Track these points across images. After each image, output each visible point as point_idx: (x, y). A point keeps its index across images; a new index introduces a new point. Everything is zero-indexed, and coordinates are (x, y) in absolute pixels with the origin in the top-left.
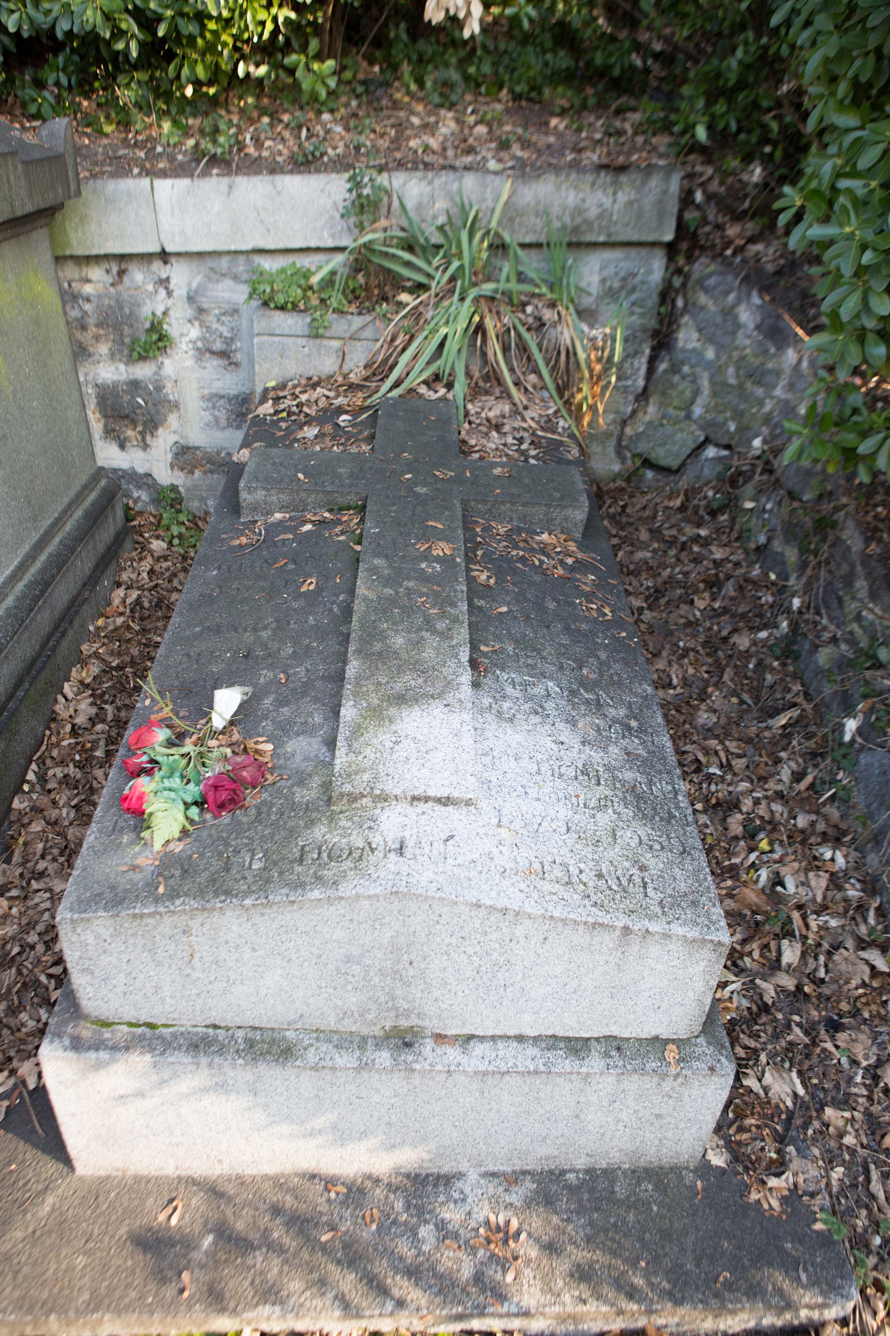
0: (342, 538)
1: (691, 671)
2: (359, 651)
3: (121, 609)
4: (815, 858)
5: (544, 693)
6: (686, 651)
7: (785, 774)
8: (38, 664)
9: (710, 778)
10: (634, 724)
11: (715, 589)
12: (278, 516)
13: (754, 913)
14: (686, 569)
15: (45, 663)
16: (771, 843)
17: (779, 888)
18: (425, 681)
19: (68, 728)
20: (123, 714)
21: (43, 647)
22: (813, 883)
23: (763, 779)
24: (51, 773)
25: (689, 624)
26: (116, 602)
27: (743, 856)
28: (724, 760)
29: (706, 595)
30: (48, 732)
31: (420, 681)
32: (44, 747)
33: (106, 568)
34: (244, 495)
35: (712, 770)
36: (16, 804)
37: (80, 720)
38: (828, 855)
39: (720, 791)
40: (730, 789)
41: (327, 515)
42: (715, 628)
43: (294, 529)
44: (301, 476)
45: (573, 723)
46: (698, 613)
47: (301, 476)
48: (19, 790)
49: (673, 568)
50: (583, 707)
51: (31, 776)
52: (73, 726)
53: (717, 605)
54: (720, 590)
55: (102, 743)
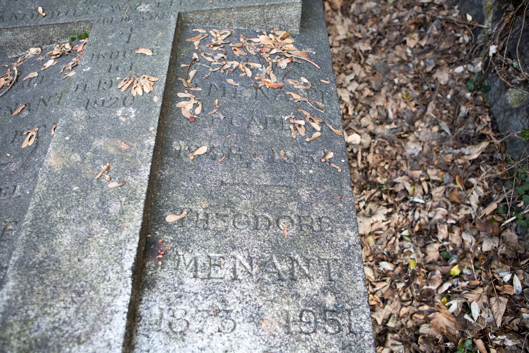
1: (403, 105)
2: (20, 263)
4: (497, 282)
5: (229, 275)
6: (401, 86)
7: (474, 200)
9: (414, 205)
10: (330, 301)
11: (422, 30)
13: (446, 340)
14: (401, 14)
16: (461, 268)
17: (466, 317)
18: (77, 312)
22: (494, 308)
23: (457, 205)
25: (402, 62)
27: (438, 284)
28: (426, 190)
29: (416, 35)
31: (73, 309)
35: (416, 200)
38: (507, 277)
39: (422, 216)
40: (430, 215)
42: (422, 63)
44: (40, 9)
45: (256, 319)
46: (409, 51)
47: (40, 9)
49: (391, 14)
50: (272, 288)
53: (423, 43)
54: (426, 29)
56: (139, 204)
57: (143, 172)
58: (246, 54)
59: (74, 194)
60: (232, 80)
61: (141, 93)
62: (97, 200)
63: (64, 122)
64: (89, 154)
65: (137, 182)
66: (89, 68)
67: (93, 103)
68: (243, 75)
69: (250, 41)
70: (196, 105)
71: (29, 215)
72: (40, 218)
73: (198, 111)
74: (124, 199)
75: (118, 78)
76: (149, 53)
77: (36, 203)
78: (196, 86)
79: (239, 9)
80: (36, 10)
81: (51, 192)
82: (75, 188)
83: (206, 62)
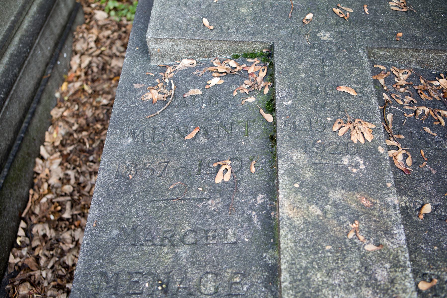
0: (251, 99)
3: (78, 73)
8: (14, 148)
12: (186, 63)
15: (20, 146)
19: (45, 186)
20: (82, 179)
21: (16, 133)
24: (34, 230)
26: (75, 67)
30: (31, 192)
32: (29, 204)
33: (63, 45)
34: (151, 45)
36: (12, 260)
37: (54, 181)
41: (233, 63)
43: (202, 82)
44: (205, 21)
47: (205, 21)
48: (13, 244)
51: (21, 232)
52: (49, 185)
55: (68, 206)
56: (407, 272)
57: (398, 235)
58: (431, 99)
59: (329, 254)
60: (428, 129)
61: (362, 141)
62: (358, 264)
63: (286, 165)
64: (328, 207)
65: (395, 247)
66: (290, 102)
67: (310, 146)
68: (437, 123)
69: (431, 85)
70: (405, 156)
71: (285, 276)
72: (300, 280)
73: (409, 161)
74: (388, 265)
75: (329, 119)
76: (353, 93)
77: (288, 261)
78: (398, 134)
79: (428, 51)
80: (200, 20)
81: (300, 249)
82: (328, 248)
83: (397, 105)
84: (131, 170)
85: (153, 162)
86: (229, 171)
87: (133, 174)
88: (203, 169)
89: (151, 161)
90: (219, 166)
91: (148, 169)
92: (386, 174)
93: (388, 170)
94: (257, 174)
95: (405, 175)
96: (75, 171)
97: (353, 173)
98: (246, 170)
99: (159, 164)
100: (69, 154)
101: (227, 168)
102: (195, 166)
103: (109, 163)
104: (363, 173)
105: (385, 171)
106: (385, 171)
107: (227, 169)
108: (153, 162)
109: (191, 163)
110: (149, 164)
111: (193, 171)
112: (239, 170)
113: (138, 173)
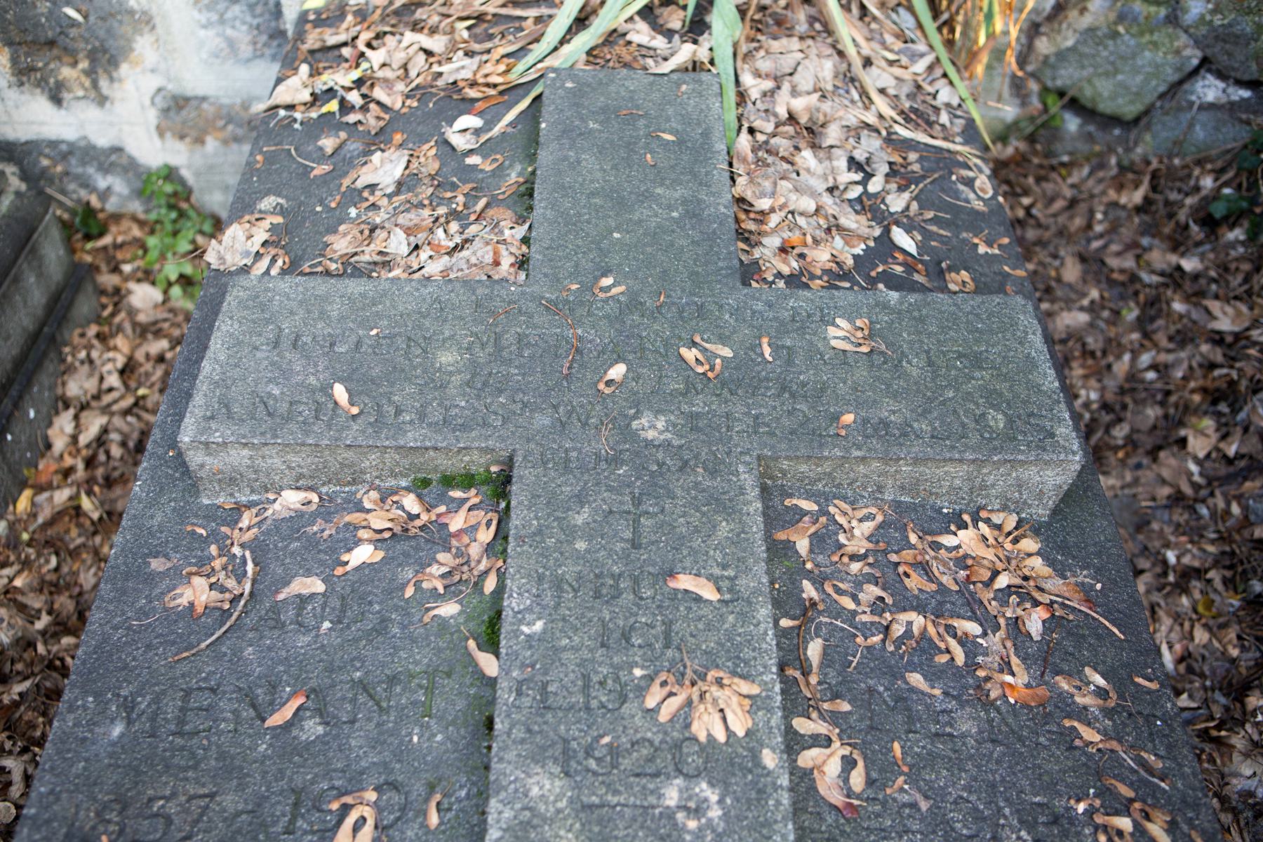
0: (449, 609)
1: (1201, 636)
3: (69, 461)
6: (1188, 574)
11: (1223, 407)
12: (292, 499)
14: (1164, 358)
25: (1178, 498)
26: (59, 444)
29: (1208, 423)
33: (28, 384)
34: (195, 458)
41: (411, 503)
42: (1235, 509)
43: (325, 555)
44: (340, 392)
46: (1193, 468)
47: (340, 392)
49: (1135, 355)
53: (1232, 450)
54: (1235, 411)
58: (934, 587)
60: (918, 676)
61: (721, 737)
63: (508, 814)
66: (539, 626)
67: (581, 755)
68: (944, 659)
69: (936, 546)
70: (848, 764)
73: (857, 779)
75: (638, 672)
76: (709, 593)
78: (836, 696)
79: (916, 461)
80: (326, 389)
83: (839, 612)
84: (109, 822)
85: (174, 795)
86: (370, 822)
87: (112, 833)
88: (303, 816)
89: (168, 793)
90: (346, 809)
91: (157, 815)
92: (775, 832)
93: (783, 818)
94: (444, 832)
95: (842, 821)
96: (26, 757)
97: (689, 832)
98: (414, 821)
99: (188, 801)
100: (16, 705)
101: (365, 814)
102: (283, 808)
103: (51, 798)
104: (713, 831)
105: (776, 822)
106: (776, 822)
107: (364, 819)
108: (174, 795)
109: (274, 799)
110: (161, 802)
111: (275, 823)
112: (398, 819)
113: (128, 830)
